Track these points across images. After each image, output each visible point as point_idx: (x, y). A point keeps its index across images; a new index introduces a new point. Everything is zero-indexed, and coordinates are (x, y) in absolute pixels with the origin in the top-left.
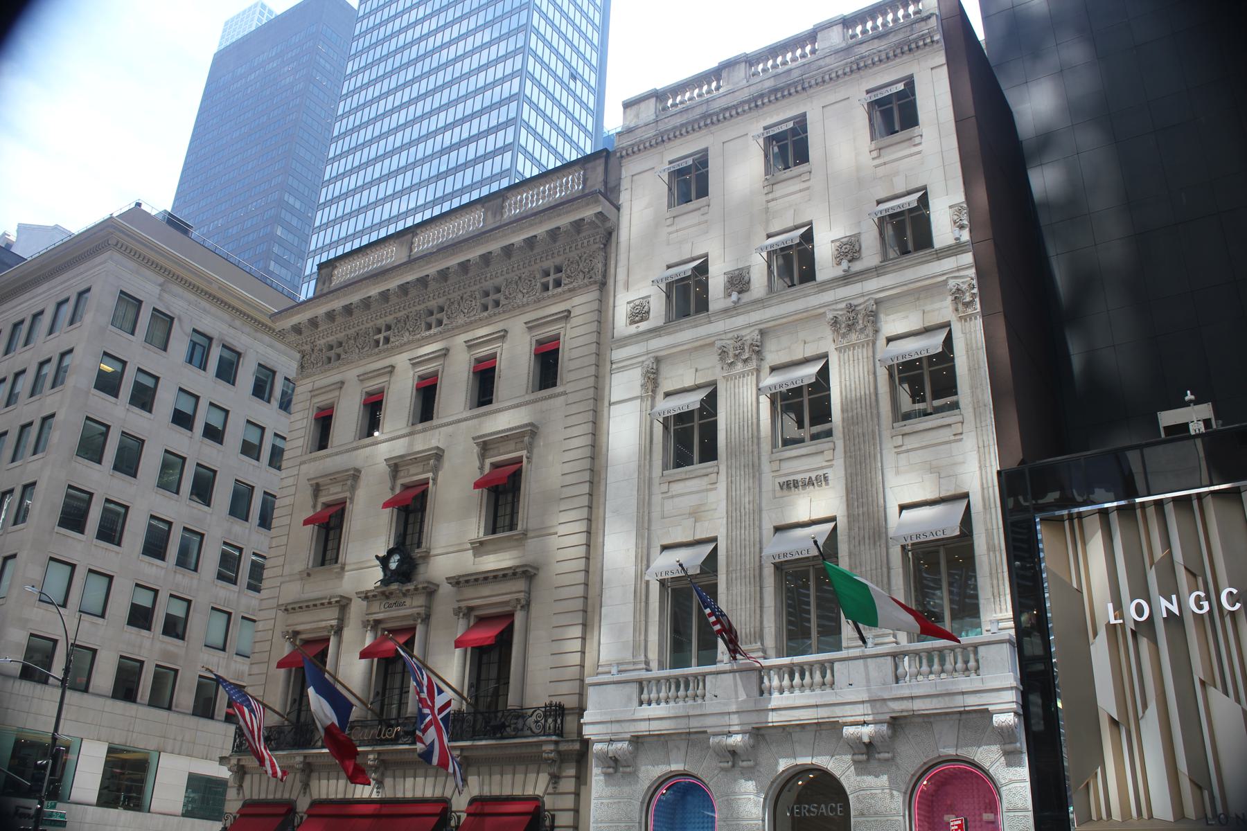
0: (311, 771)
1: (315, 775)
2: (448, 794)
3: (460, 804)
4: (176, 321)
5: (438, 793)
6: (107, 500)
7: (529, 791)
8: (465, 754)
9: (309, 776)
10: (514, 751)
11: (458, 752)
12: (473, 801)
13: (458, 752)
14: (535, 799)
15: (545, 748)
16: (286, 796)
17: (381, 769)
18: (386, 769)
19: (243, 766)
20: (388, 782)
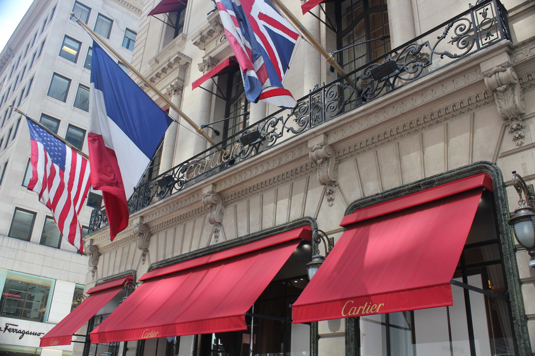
0: (151, 235)
1: (154, 239)
2: (310, 212)
3: (330, 219)
4: (114, 22)
5: (296, 215)
6: (70, 125)
7: (460, 160)
8: (332, 140)
9: (148, 241)
10: (419, 101)
11: (321, 139)
12: (355, 207)
13: (321, 139)
14: (480, 168)
15: (487, 66)
16: (129, 268)
17: (219, 206)
18: (225, 205)
19: (96, 246)
20: (228, 221)
